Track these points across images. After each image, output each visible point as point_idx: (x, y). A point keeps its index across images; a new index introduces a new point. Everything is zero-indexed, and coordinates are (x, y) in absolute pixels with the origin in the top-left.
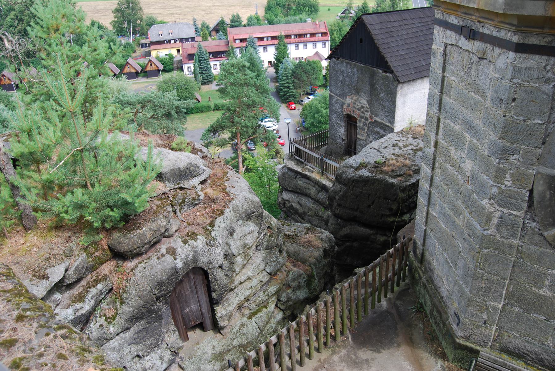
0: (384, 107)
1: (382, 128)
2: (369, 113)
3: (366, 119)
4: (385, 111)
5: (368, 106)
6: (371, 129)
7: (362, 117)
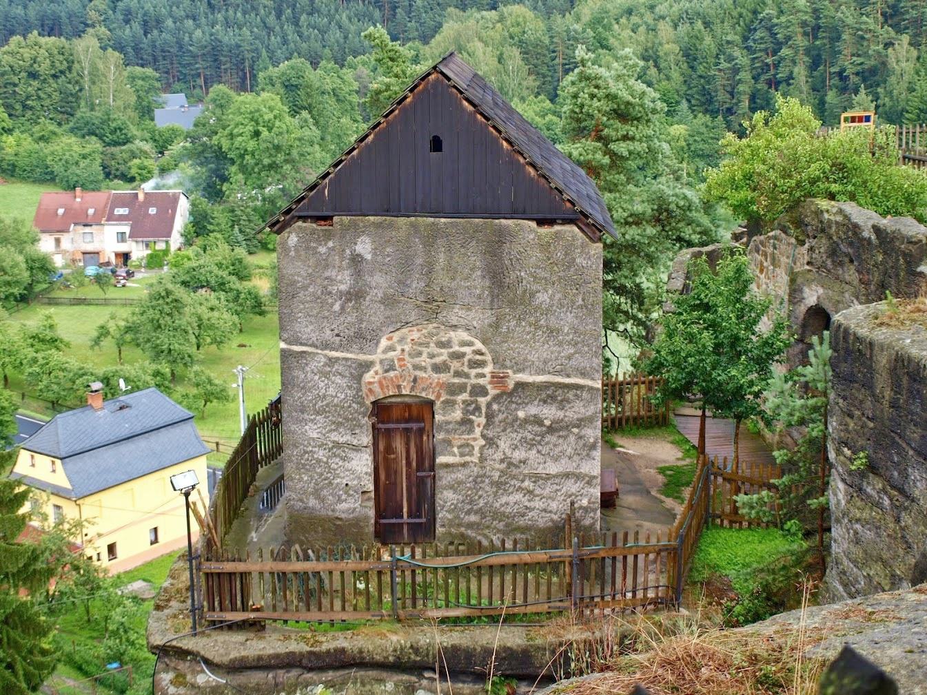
0: (552, 332)
1: (549, 400)
2: (488, 370)
3: (480, 391)
4: (560, 344)
5: (479, 345)
6: (501, 417)
7: (454, 390)
